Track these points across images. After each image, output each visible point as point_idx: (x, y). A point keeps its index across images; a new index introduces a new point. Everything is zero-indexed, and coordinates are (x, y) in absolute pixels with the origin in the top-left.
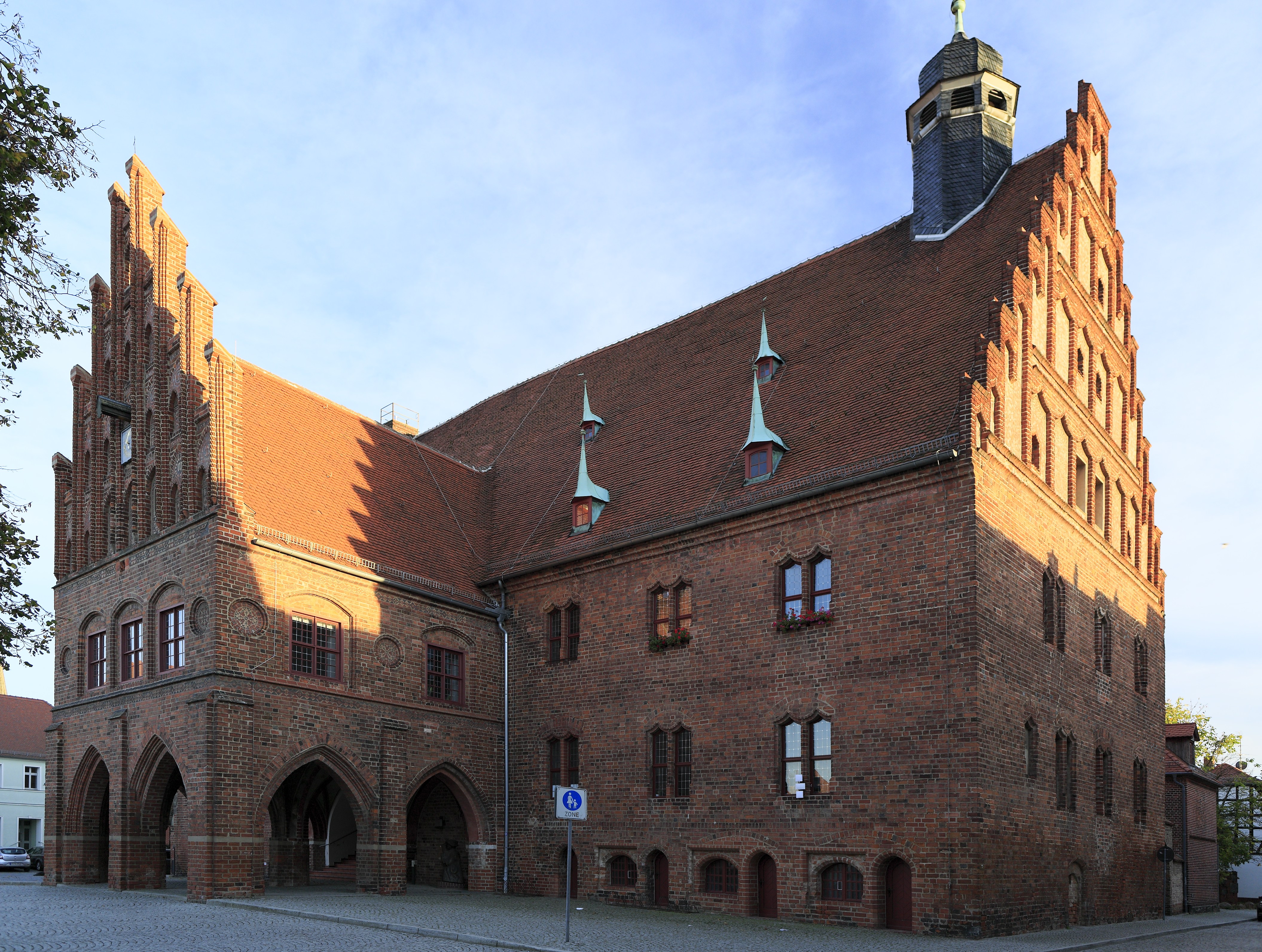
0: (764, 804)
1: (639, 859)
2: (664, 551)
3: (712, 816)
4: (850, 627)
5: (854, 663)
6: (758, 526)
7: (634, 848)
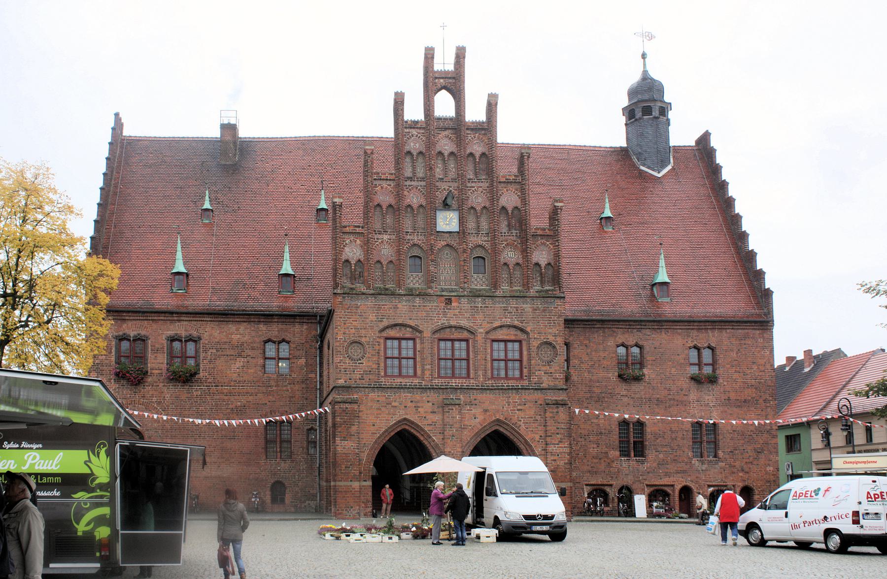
0: (687, 462)
2: (628, 327)
4: (725, 383)
5: (728, 400)
6: (681, 327)
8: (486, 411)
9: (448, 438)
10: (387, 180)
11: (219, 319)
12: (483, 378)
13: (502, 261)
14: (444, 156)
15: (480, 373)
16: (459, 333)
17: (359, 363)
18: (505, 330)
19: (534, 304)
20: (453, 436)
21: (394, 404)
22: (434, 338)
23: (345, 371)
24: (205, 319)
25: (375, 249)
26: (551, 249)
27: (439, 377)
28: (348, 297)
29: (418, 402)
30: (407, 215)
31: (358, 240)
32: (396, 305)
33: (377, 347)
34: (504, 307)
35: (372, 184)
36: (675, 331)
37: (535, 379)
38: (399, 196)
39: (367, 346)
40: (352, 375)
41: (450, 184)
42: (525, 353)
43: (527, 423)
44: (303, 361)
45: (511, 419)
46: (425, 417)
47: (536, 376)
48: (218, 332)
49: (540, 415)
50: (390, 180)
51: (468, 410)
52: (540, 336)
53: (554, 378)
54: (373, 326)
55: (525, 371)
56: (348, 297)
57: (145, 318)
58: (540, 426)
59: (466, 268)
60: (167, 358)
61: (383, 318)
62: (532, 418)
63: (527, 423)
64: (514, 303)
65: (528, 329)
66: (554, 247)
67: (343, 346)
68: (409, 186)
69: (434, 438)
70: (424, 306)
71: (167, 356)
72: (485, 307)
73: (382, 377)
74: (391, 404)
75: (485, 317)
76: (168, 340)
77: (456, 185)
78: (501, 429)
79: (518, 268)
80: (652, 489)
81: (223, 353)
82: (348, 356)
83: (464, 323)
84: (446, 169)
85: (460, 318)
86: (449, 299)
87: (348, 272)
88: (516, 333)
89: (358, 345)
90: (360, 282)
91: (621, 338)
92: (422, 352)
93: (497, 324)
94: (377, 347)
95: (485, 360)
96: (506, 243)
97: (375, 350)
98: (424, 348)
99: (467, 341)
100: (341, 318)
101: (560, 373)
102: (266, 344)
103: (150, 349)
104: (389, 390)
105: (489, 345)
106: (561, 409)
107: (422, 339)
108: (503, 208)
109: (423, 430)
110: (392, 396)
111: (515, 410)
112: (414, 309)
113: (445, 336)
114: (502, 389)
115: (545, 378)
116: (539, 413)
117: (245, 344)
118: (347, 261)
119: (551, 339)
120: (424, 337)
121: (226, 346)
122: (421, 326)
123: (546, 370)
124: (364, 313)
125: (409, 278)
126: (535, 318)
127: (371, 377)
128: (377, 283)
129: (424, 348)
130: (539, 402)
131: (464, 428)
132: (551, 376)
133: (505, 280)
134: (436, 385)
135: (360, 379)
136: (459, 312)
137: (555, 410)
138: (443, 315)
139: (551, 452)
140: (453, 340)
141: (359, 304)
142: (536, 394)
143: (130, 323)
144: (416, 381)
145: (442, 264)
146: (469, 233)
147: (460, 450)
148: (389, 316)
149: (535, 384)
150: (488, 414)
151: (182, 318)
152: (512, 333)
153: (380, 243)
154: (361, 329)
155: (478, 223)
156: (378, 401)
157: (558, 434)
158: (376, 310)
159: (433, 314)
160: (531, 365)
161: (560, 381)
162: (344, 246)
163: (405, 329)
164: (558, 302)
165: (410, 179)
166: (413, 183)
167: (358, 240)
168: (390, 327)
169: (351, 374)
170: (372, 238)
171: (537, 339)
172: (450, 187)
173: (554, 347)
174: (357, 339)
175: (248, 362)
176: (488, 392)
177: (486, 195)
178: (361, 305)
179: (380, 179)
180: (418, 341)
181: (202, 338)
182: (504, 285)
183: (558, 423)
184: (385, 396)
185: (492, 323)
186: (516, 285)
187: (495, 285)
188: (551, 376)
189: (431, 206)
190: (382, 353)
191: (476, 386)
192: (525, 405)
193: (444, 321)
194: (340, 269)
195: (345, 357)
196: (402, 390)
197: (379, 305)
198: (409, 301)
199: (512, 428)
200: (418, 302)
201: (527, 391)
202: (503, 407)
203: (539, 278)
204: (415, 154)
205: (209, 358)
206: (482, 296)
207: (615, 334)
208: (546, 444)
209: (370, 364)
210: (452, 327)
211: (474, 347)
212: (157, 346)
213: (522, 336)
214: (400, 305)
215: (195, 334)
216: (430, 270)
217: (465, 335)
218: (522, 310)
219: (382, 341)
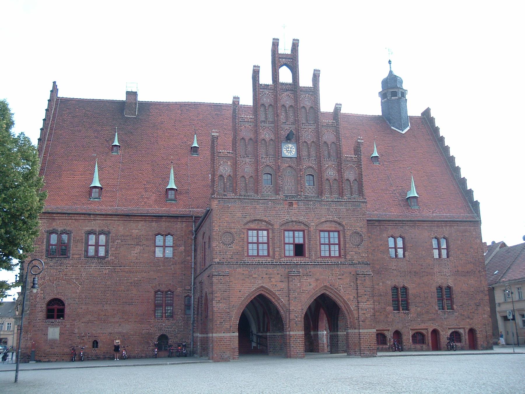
1: (389, 335)
3: (418, 318)
7: (388, 330)
8: (317, 280)
9: (292, 300)
10: (248, 122)
11: (124, 219)
13: (326, 177)
14: (286, 108)
16: (298, 225)
18: (328, 224)
19: (346, 206)
21: (254, 276)
22: (281, 229)
23: (220, 253)
24: (113, 219)
27: (285, 256)
28: (222, 200)
29: (270, 274)
31: (229, 162)
32: (255, 207)
33: (242, 236)
34: (327, 208)
36: (424, 227)
37: (349, 257)
38: (256, 132)
39: (235, 235)
40: (225, 256)
41: (290, 126)
42: (342, 239)
43: (345, 288)
44: (182, 248)
45: (334, 285)
46: (276, 285)
47: (350, 255)
48: (123, 228)
49: (353, 282)
50: (251, 122)
51: (305, 279)
52: (351, 228)
53: (361, 257)
54: (240, 221)
55: (342, 251)
56: (222, 200)
57: (69, 218)
58: (353, 289)
60: (85, 247)
63: (345, 288)
64: (334, 206)
65: (344, 223)
66: (358, 168)
67: (219, 235)
68: (263, 126)
69: (282, 300)
70: (275, 207)
71: (85, 245)
72: (315, 208)
73: (245, 257)
74: (252, 276)
75: (315, 215)
76: (86, 234)
77: (294, 126)
78: (327, 293)
79: (335, 182)
80: (414, 332)
81: (126, 243)
82: (222, 242)
83: (301, 219)
84: (287, 116)
85: (298, 215)
86: (291, 202)
88: (335, 226)
89: (229, 234)
90: (230, 190)
91: (391, 232)
92: (273, 239)
93: (323, 219)
95: (316, 244)
97: (241, 238)
98: (274, 236)
100: (217, 215)
101: (365, 253)
102: (156, 236)
103: (72, 240)
104: (251, 266)
106: (367, 278)
107: (273, 230)
108: (325, 142)
109: (274, 294)
114: (327, 264)
115: (355, 257)
116: (353, 281)
117: (142, 237)
118: (221, 176)
119: (359, 229)
120: (274, 229)
121: (128, 238)
122: (273, 221)
124: (233, 212)
125: (263, 188)
126: (348, 216)
129: (274, 236)
130: (352, 273)
131: (302, 293)
132: (360, 255)
133: (327, 190)
134: (283, 262)
135: (230, 258)
137: (363, 279)
141: (230, 205)
142: (350, 268)
143: (58, 222)
144: (269, 259)
145: (286, 179)
146: (303, 159)
147: (300, 308)
148: (250, 214)
150: (319, 282)
151: (97, 218)
153: (244, 164)
154: (231, 223)
155: (309, 152)
156: (243, 274)
157: (365, 295)
158: (242, 210)
159: (281, 213)
160: (346, 248)
161: (365, 259)
163: (262, 223)
164: (362, 205)
166: (265, 125)
167: (229, 162)
168: (251, 222)
170: (239, 161)
171: (349, 229)
172: (291, 128)
173: (361, 235)
174: (228, 230)
175: (144, 249)
176: (318, 266)
177: (314, 134)
178: (231, 206)
179: (244, 121)
180: (270, 231)
181: (111, 232)
182: (326, 193)
183: (366, 287)
184: (248, 270)
185: (320, 219)
186: (334, 193)
187: (321, 193)
188: (360, 255)
189: (278, 140)
190: (245, 240)
191: (311, 262)
192: (343, 275)
193: (288, 218)
195: (220, 243)
196: (260, 266)
197: (244, 206)
198: (264, 203)
199: (336, 292)
201: (344, 265)
202: (329, 277)
203: (349, 189)
204: (267, 106)
205: (115, 247)
206: (313, 201)
207: (387, 229)
209: (238, 247)
210: (293, 222)
211: (308, 235)
212: (78, 238)
213: (341, 228)
214: (258, 207)
215: (106, 229)
216: (278, 183)
217: (302, 227)
218: (339, 210)
219: (245, 231)
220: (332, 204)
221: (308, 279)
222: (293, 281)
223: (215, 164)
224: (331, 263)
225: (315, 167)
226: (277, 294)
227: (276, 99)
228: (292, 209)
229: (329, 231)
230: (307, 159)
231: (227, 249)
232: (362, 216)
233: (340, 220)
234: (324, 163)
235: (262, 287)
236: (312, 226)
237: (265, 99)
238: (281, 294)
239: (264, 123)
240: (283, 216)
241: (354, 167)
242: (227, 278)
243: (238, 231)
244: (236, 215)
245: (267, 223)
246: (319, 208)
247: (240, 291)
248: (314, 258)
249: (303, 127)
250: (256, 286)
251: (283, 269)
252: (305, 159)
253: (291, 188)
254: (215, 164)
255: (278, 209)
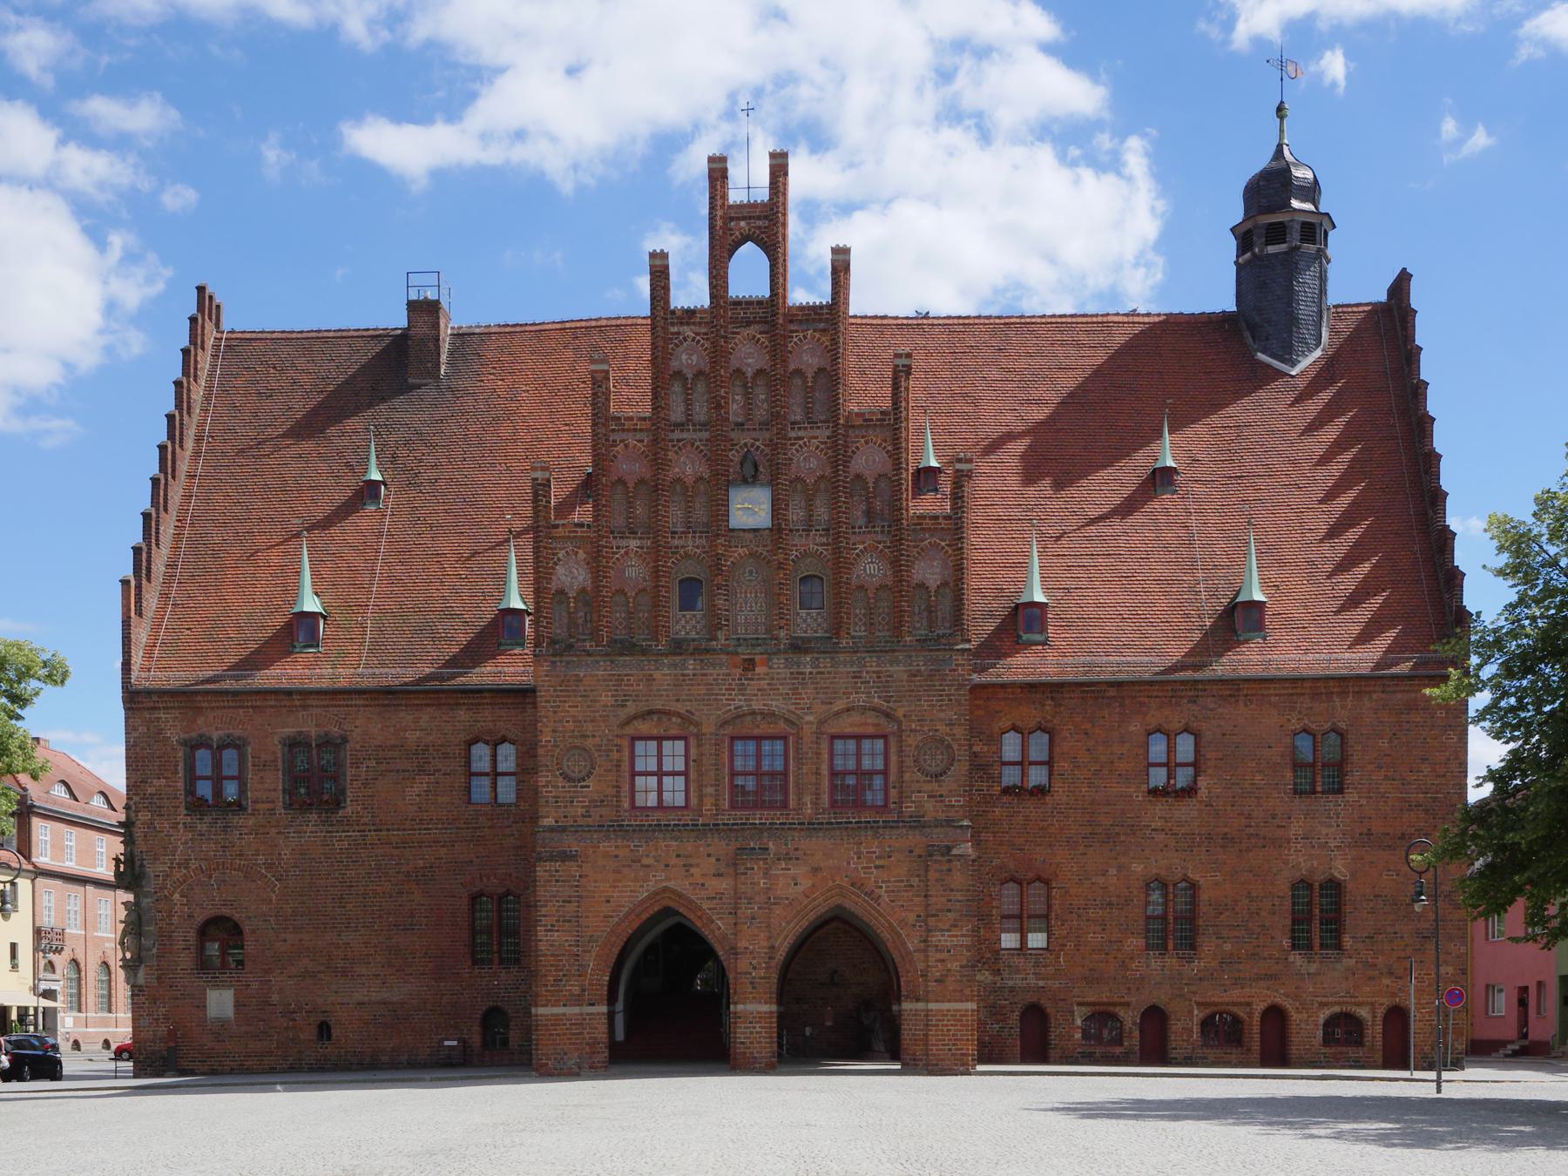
8: (816, 870)
12: (812, 808)
15: (807, 799)
17: (582, 787)
18: (856, 718)
20: (753, 918)
21: (645, 861)
22: (723, 735)
23: (557, 802)
25: (612, 568)
26: (950, 556)
30: (676, 499)
31: (581, 551)
32: (651, 675)
35: (607, 440)
37: (910, 808)
42: (893, 758)
46: (703, 885)
50: (641, 430)
55: (893, 793)
59: (783, 599)
61: (627, 700)
62: (902, 881)
64: (874, 664)
67: (552, 756)
68: (678, 441)
69: (719, 922)
74: (639, 861)
75: (817, 693)
82: (561, 774)
83: (777, 704)
84: (749, 404)
87: (564, 614)
88: (876, 721)
93: (839, 705)
94: (615, 755)
96: (861, 547)
97: (612, 761)
99: (784, 738)
105: (825, 746)
109: (700, 909)
110: (641, 846)
111: (871, 868)
112: (684, 680)
113: (744, 732)
114: (847, 828)
120: (703, 735)
122: (697, 713)
123: (932, 791)
124: (592, 691)
126: (912, 691)
127: (604, 811)
128: (618, 632)
131: (775, 904)
134: (724, 824)
136: (769, 684)
138: (739, 690)
139: (937, 946)
140: (759, 739)
141: (582, 674)
146: (791, 531)
147: (765, 944)
149: (911, 817)
152: (869, 721)
153: (622, 555)
156: (616, 856)
158: (614, 685)
162: (556, 564)
165: (680, 426)
167: (581, 551)
169: (566, 807)
170: (607, 547)
172: (758, 440)
178: (585, 676)
182: (857, 628)
185: (831, 703)
186: (880, 628)
187: (837, 628)
190: (625, 766)
194: (545, 608)
197: (619, 675)
200: (691, 667)
202: (849, 863)
204: (690, 376)
208: (929, 931)
216: (715, 606)
217: (782, 726)
219: (626, 743)
220: (868, 659)
221: (790, 869)
222: (746, 874)
223: (541, 562)
224: (855, 826)
225: (825, 553)
226: (705, 907)
227: (718, 355)
228: (752, 679)
229: (858, 738)
230: (803, 530)
231: (574, 792)
232: (956, 690)
233: (891, 705)
234: (853, 539)
235: (665, 889)
236: (807, 723)
237: (684, 357)
238: (715, 909)
239: (682, 431)
240: (727, 700)
241: (943, 548)
242: (572, 867)
243: (605, 742)
244: (598, 701)
245: (682, 718)
246: (829, 673)
247: (608, 901)
248: (809, 811)
249: (793, 434)
250: (652, 886)
251: (723, 843)
252: (798, 530)
253: (756, 619)
254: (541, 562)
255: (714, 680)
